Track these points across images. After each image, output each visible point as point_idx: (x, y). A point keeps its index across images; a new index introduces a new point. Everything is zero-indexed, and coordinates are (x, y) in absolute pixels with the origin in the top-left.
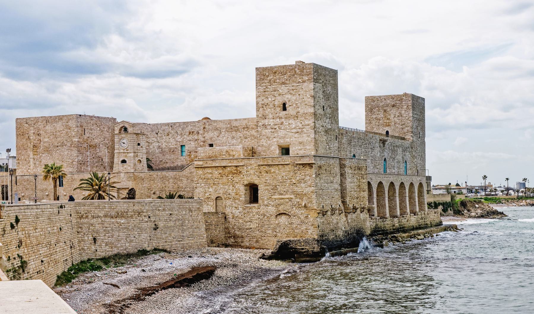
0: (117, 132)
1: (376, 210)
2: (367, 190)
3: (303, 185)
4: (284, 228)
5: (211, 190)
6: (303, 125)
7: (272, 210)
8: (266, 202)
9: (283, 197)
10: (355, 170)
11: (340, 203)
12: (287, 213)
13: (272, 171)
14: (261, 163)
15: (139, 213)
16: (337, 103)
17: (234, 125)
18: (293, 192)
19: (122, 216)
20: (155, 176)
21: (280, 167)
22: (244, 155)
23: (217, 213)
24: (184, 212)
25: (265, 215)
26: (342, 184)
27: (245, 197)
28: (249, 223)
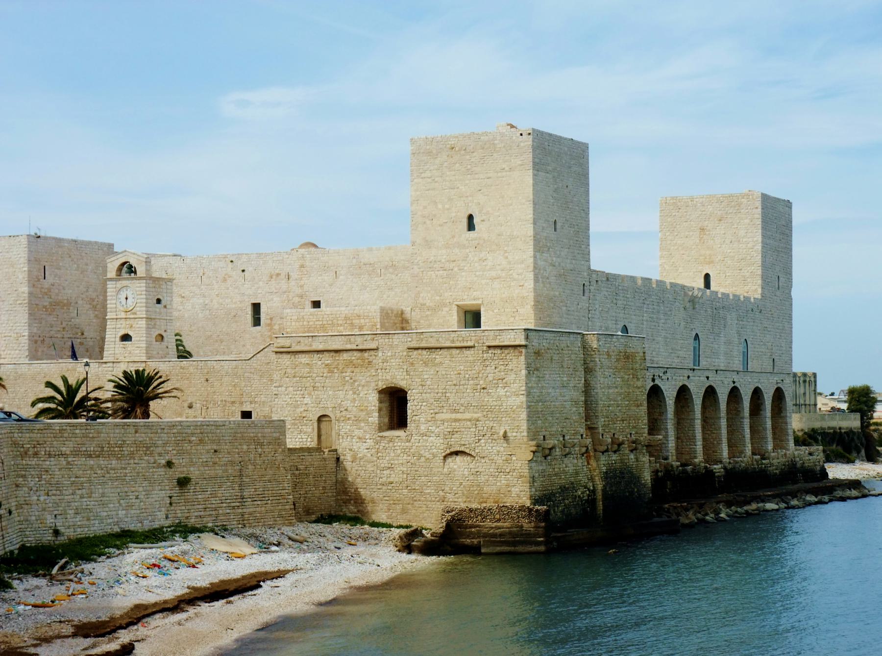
0: (112, 273)
1: (672, 444)
2: (645, 403)
3: (502, 392)
4: (461, 484)
5: (307, 400)
6: (509, 263)
7: (437, 445)
8: (423, 428)
9: (459, 416)
10: (618, 360)
11: (582, 430)
12: (467, 451)
13: (437, 361)
14: (414, 344)
15: (148, 448)
16: (588, 214)
18: (481, 407)
19: (111, 455)
20: (191, 370)
21: (454, 352)
22: (383, 325)
23: (319, 449)
24: (245, 447)
25: (421, 456)
26: (587, 390)
27: (380, 417)
28: (388, 472)
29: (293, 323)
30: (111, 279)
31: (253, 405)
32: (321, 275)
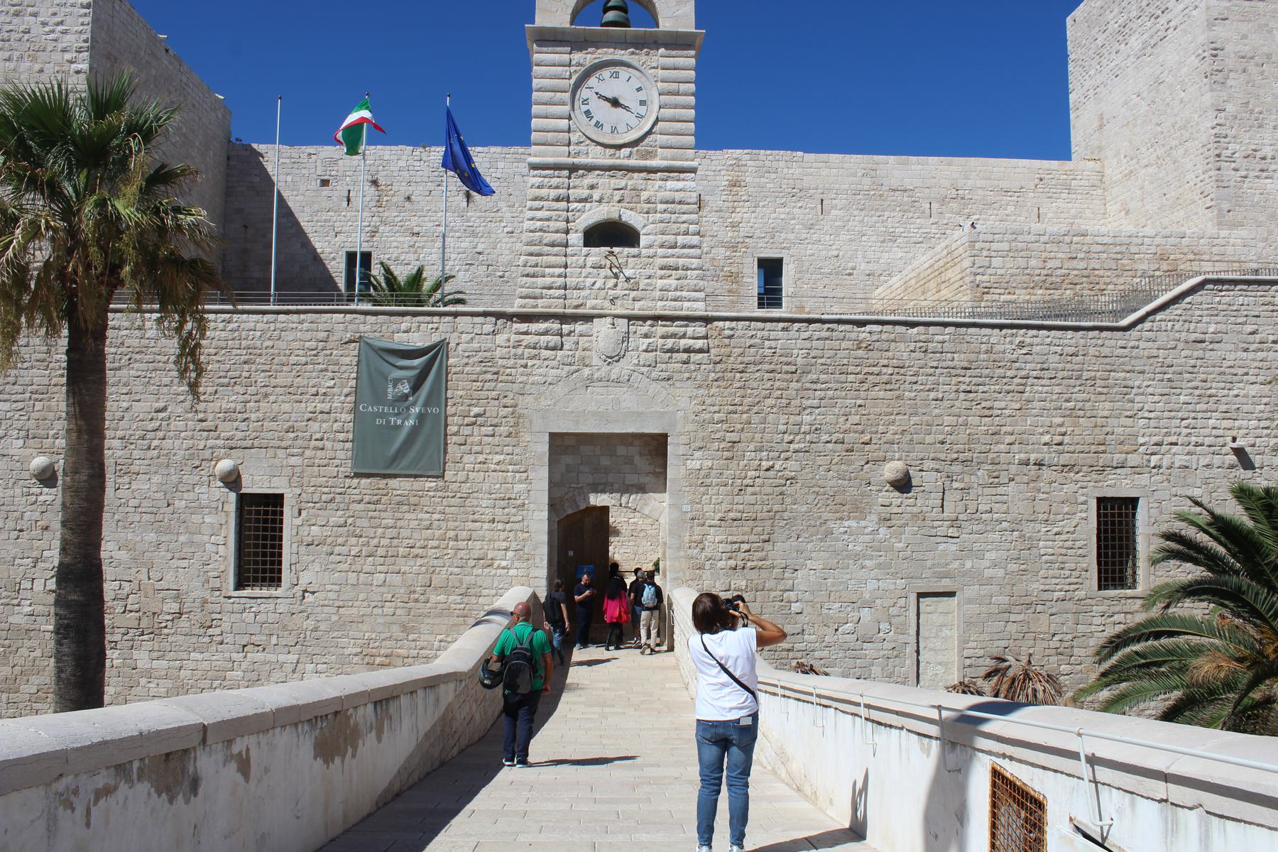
17: (895, 183)
20: (901, 351)
29: (996, 262)
30: (551, 38)
31: (1144, 479)
32: (784, 205)
